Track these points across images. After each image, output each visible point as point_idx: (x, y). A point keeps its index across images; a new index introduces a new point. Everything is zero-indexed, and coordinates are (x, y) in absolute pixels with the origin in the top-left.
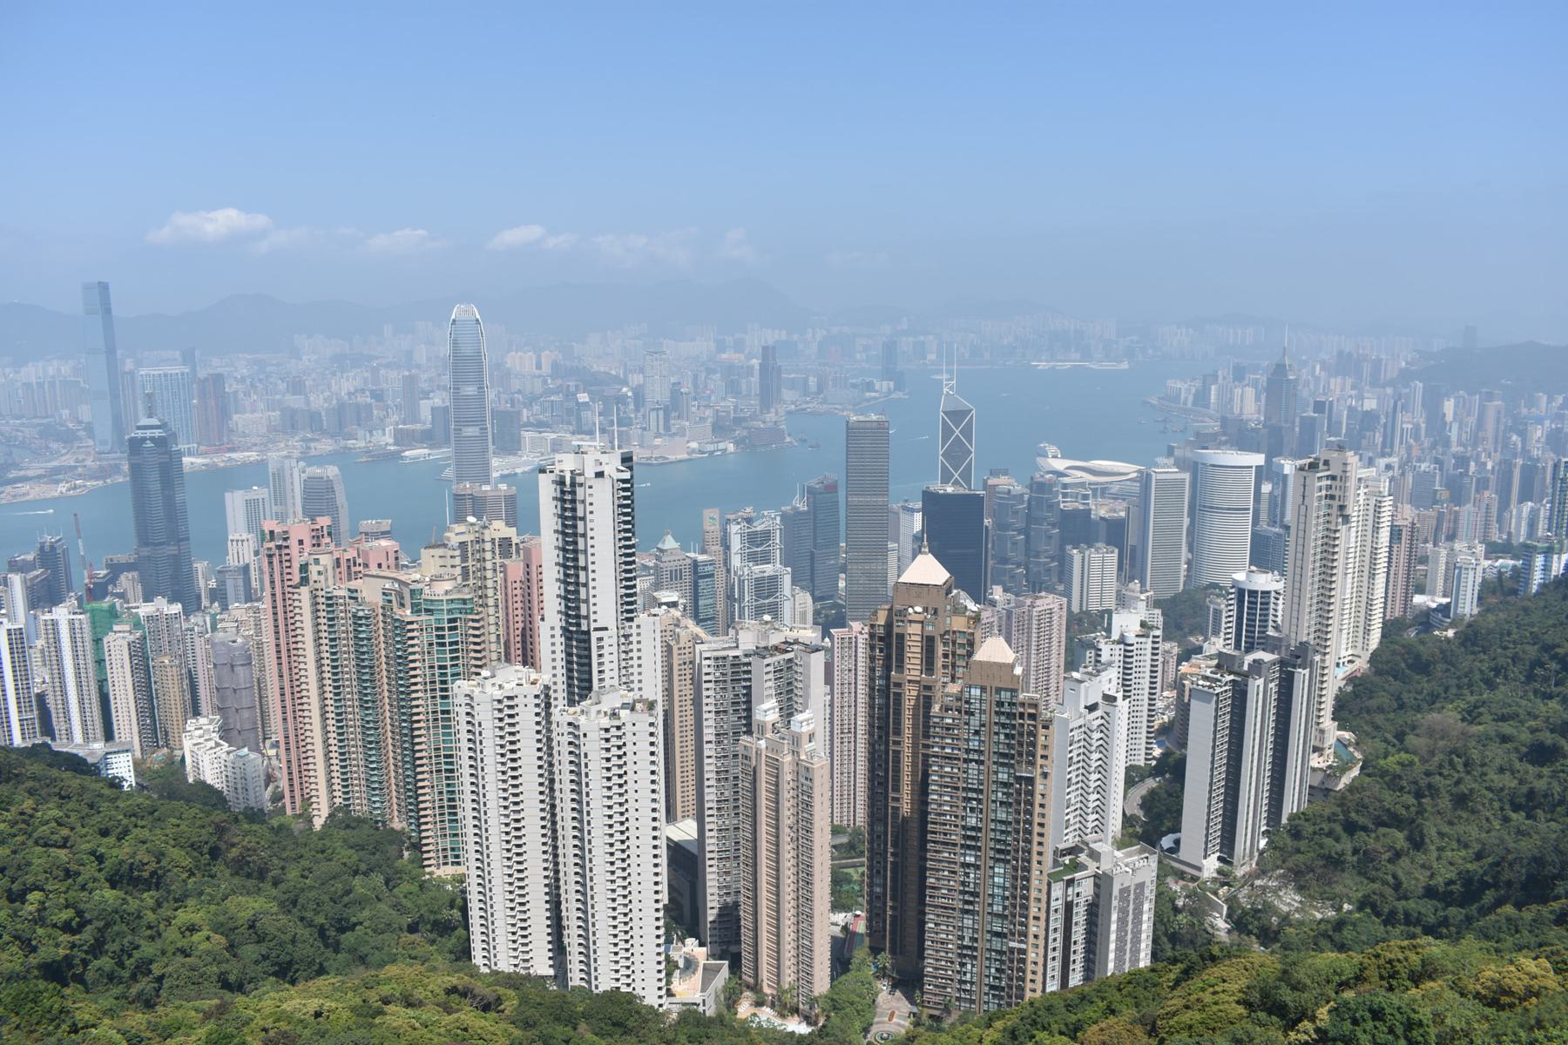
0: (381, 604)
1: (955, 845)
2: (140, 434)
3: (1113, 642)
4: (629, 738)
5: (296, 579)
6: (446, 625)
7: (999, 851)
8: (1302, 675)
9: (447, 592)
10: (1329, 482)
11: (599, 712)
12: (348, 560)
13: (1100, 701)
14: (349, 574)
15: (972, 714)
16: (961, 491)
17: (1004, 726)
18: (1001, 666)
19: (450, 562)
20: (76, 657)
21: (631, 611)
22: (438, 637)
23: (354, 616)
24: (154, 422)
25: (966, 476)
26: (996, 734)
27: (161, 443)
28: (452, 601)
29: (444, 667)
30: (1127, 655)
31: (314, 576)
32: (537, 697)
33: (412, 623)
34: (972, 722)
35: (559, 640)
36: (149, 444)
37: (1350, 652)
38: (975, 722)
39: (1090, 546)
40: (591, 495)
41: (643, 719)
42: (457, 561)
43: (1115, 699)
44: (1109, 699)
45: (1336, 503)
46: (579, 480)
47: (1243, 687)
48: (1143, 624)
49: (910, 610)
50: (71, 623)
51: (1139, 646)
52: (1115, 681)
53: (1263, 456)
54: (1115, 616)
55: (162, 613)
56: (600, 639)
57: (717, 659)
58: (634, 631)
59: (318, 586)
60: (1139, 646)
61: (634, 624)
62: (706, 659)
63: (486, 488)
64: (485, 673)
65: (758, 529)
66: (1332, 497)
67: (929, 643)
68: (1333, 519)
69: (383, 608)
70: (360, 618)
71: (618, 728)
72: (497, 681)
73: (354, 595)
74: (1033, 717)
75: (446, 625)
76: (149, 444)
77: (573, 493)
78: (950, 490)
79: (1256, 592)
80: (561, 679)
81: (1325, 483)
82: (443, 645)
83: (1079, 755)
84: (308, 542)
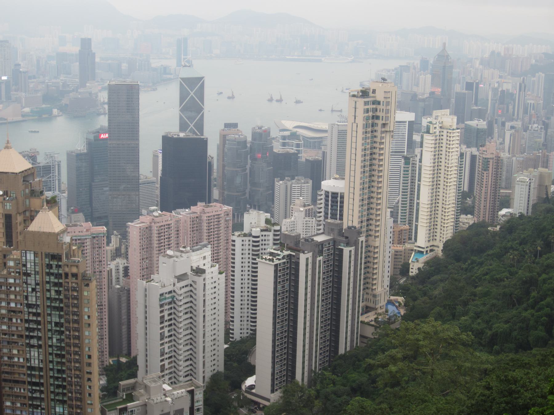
1: (24, 382)
3: (245, 235)
7: (58, 386)
8: (346, 251)
10: (374, 106)
13: (189, 272)
15: (27, 275)
16: (192, 136)
17: (56, 284)
18: (49, 235)
25: (200, 126)
26: (49, 291)
30: (256, 243)
34: (29, 282)
37: (429, 245)
38: (31, 280)
39: (293, 178)
43: (203, 271)
44: (199, 272)
45: (380, 122)
47: (297, 260)
48: (267, 221)
51: (263, 238)
52: (209, 259)
53: (413, 115)
54: (246, 216)
60: (263, 238)
65: (41, 165)
66: (378, 118)
68: (378, 134)
74: (75, 275)
78: (182, 135)
79: (337, 194)
81: (370, 107)
83: (170, 314)
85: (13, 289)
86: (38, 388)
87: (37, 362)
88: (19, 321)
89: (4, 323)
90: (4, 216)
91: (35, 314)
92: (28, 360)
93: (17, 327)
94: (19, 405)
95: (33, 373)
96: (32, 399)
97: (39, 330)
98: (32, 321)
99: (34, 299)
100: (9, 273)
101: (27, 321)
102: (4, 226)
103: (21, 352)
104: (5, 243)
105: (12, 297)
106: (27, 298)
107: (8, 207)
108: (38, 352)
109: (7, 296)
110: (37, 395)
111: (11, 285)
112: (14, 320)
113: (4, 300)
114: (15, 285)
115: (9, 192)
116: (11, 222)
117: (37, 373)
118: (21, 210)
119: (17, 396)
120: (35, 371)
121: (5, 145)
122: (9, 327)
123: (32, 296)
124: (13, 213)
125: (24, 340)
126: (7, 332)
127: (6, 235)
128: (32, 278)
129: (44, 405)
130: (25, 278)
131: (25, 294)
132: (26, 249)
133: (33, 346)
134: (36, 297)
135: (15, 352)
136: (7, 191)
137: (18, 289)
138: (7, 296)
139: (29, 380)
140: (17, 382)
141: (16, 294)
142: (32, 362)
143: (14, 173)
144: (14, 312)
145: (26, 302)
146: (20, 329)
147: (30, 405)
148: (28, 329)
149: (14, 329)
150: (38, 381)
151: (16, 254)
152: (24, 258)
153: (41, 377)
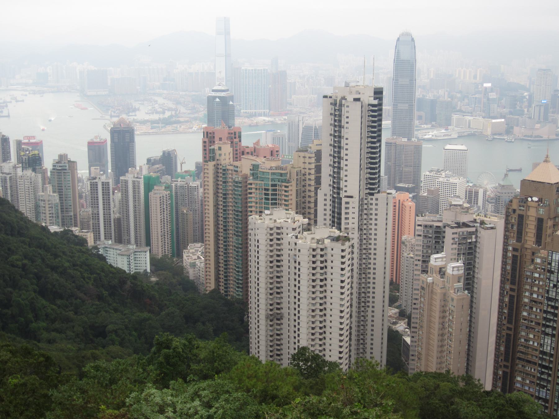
0: (249, 174)
1: (535, 364)
2: (214, 94)
4: (329, 258)
6: (270, 188)
9: (271, 168)
11: (313, 239)
15: (551, 272)
19: (307, 160)
20: (135, 201)
21: (373, 189)
22: (266, 194)
28: (273, 174)
31: (217, 157)
33: (251, 184)
34: (552, 278)
35: (329, 202)
36: (218, 100)
38: (554, 277)
40: (348, 112)
41: (338, 246)
42: (313, 160)
46: (343, 101)
49: (530, 199)
50: (134, 182)
56: (347, 203)
57: (426, 226)
58: (374, 202)
59: (219, 162)
61: (374, 197)
62: (419, 225)
63: (406, 140)
64: (267, 212)
67: (540, 221)
70: (237, 182)
71: (322, 250)
72: (273, 217)
73: (236, 169)
76: (218, 100)
77: (340, 110)
82: (268, 199)
85: (537, 282)
86: (546, 371)
87: (549, 348)
88: (538, 311)
89: (526, 311)
90: (537, 219)
91: (553, 307)
92: (541, 345)
93: (536, 316)
94: (528, 382)
95: (544, 357)
96: (540, 379)
97: (555, 321)
98: (550, 312)
99: (554, 294)
100: (536, 268)
101: (546, 312)
102: (536, 227)
103: (536, 337)
104: (535, 243)
105: (536, 289)
106: (548, 292)
107: (541, 212)
108: (552, 340)
109: (531, 288)
110: (545, 377)
111: (535, 279)
112: (534, 309)
113: (528, 290)
114: (539, 279)
115: (543, 200)
116: (542, 225)
117: (548, 358)
118: (552, 216)
119: (527, 374)
120: (546, 356)
121: (544, 159)
122: (529, 314)
123: (552, 291)
124: (545, 218)
125: (540, 327)
126: (527, 318)
127: (537, 236)
128: (555, 276)
129: (549, 387)
130: (548, 274)
131: (547, 288)
132: (552, 250)
133: (547, 334)
134: (556, 292)
135: (531, 336)
136: (542, 198)
137: (541, 283)
138: (531, 288)
139: (540, 362)
140: (529, 362)
141: (539, 287)
142: (545, 348)
143: (549, 184)
144: (535, 302)
145: (547, 295)
146: (538, 317)
147: (538, 384)
148: (545, 319)
149: (533, 316)
150: (547, 365)
151: (543, 253)
152: (550, 257)
153: (551, 362)
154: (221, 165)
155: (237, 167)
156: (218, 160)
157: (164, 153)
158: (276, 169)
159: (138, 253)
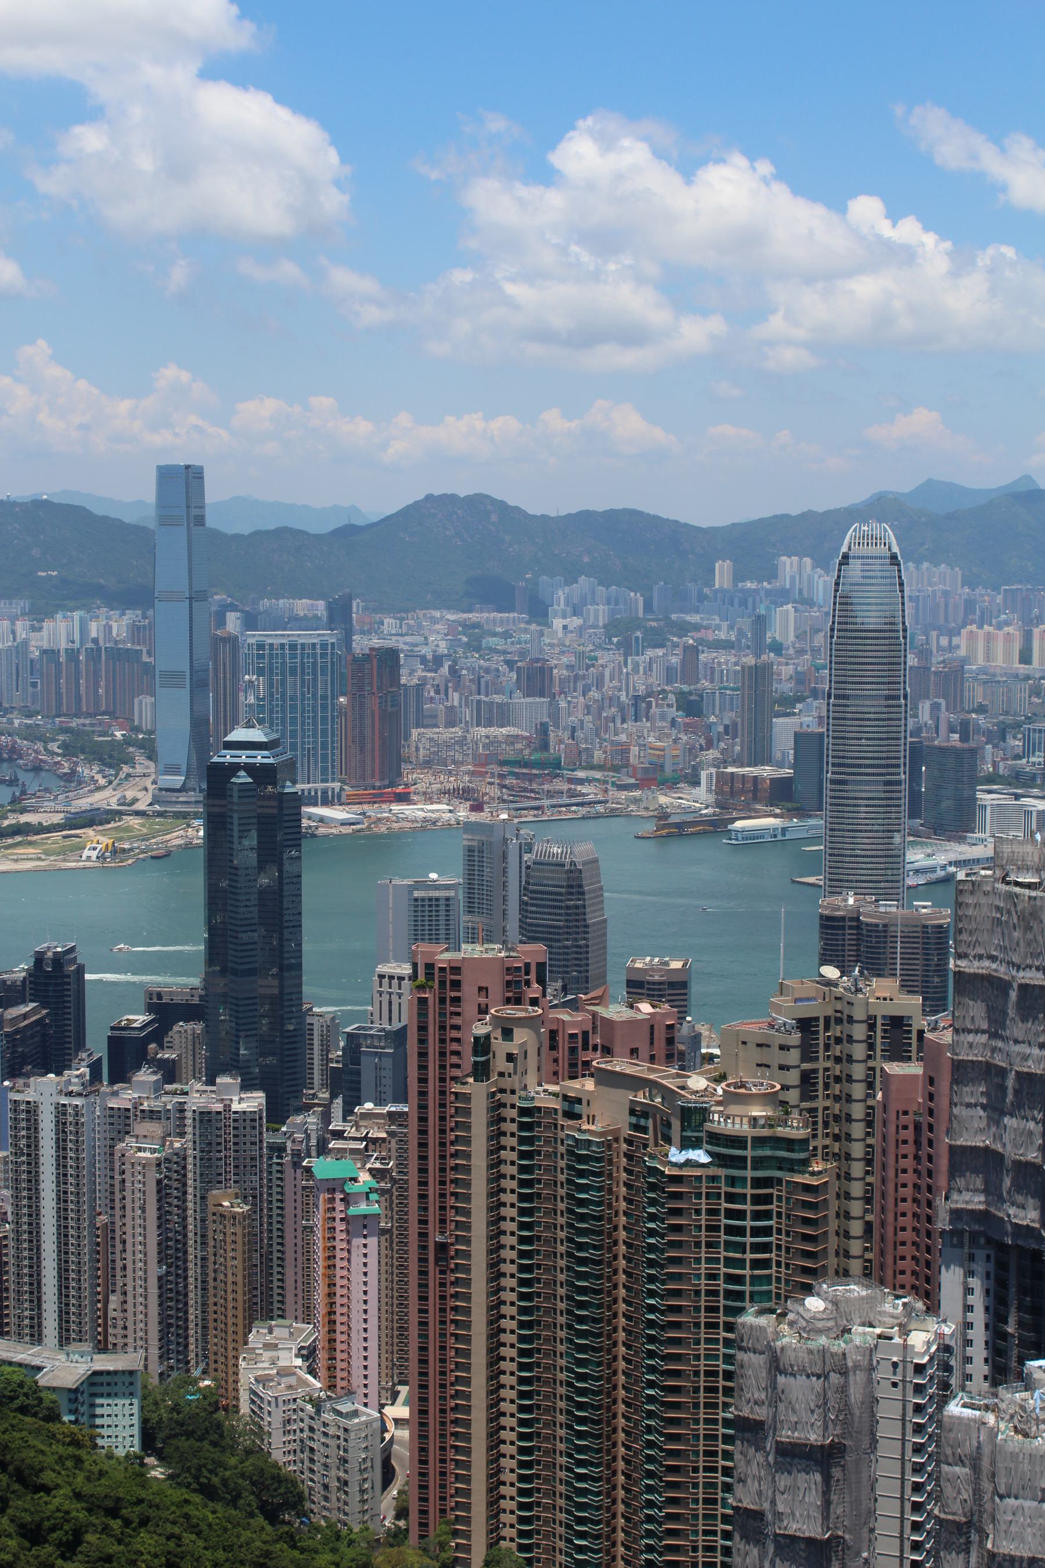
2: (228, 757)
5: (469, 1059)
6: (749, 1191)
12: (573, 1036)
14: (573, 1065)
19: (777, 1057)
20: (61, 1177)
22: (731, 1214)
23: (570, 1152)
24: (256, 735)
27: (263, 774)
29: (739, 1280)
31: (500, 1064)
32: (919, 1369)
36: (243, 778)
42: (793, 1057)
50: (61, 1110)
55: (227, 1109)
59: (506, 1083)
69: (629, 1142)
70: (581, 1159)
75: (749, 1191)
76: (243, 778)
80: (979, 1334)
82: (740, 1231)
84: (496, 990)
154: (513, 1092)
155: (579, 1101)
156: (501, 1074)
157: (39, 959)
158: (771, 1126)
159: (105, 1379)
